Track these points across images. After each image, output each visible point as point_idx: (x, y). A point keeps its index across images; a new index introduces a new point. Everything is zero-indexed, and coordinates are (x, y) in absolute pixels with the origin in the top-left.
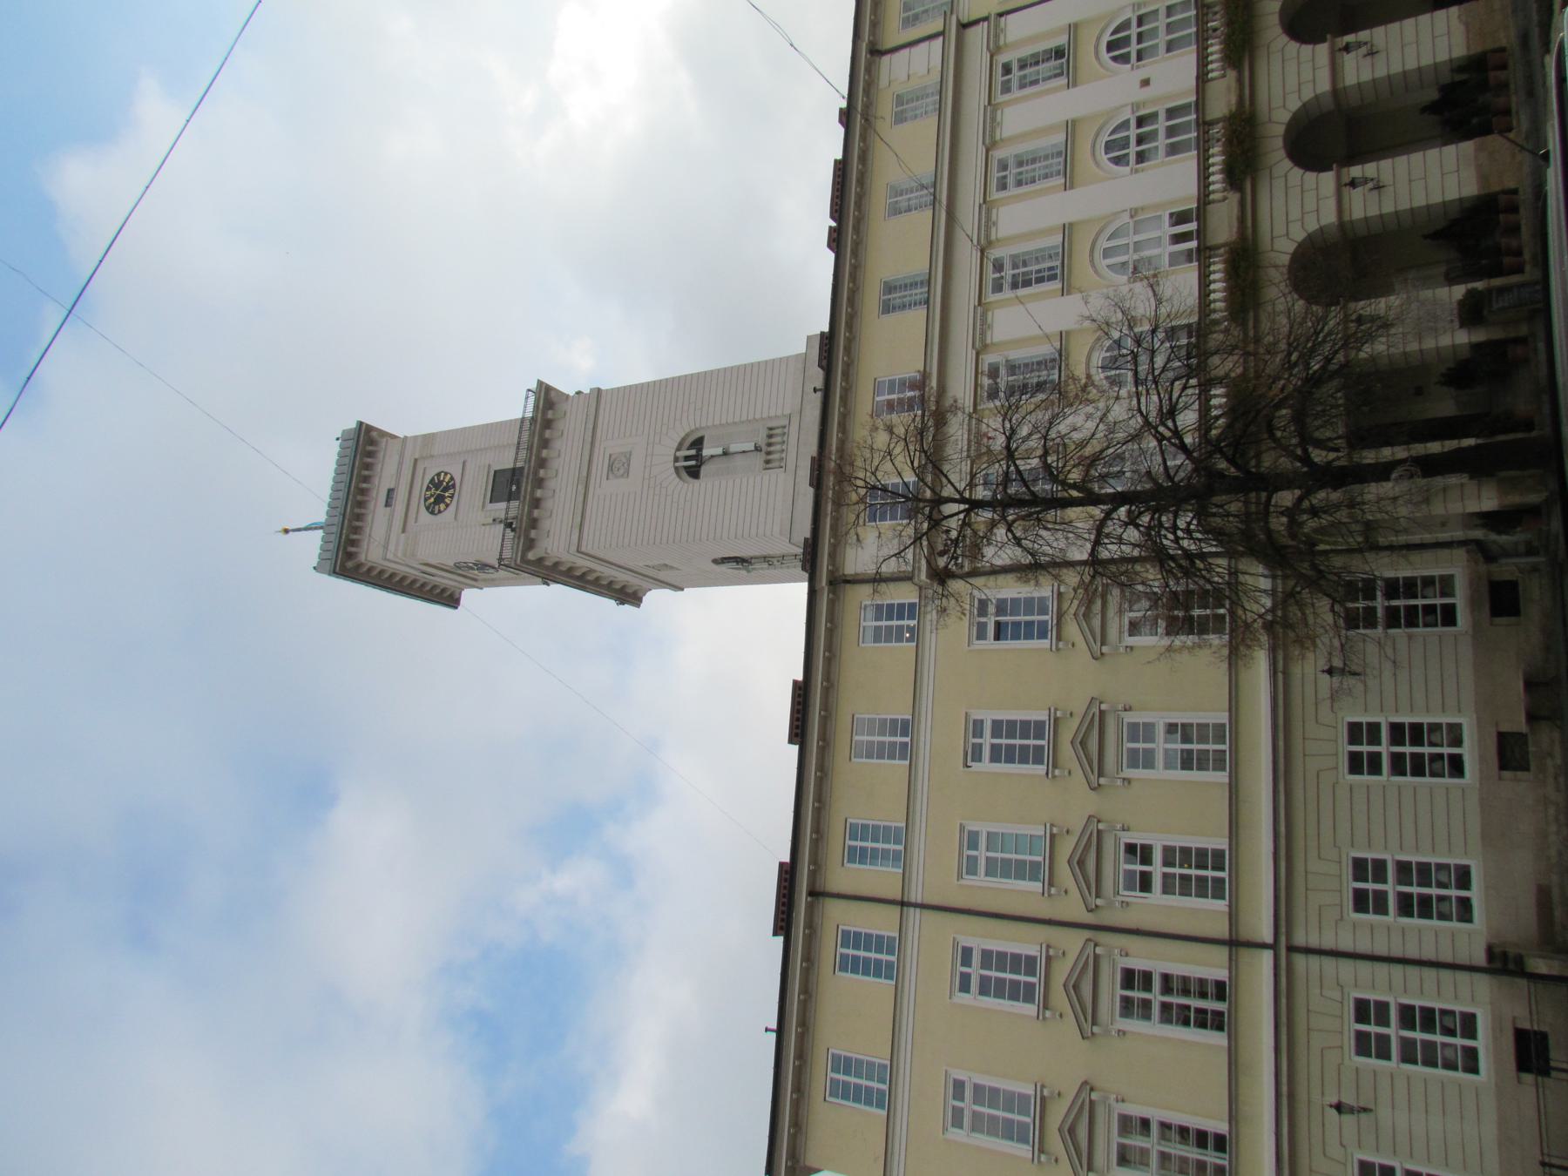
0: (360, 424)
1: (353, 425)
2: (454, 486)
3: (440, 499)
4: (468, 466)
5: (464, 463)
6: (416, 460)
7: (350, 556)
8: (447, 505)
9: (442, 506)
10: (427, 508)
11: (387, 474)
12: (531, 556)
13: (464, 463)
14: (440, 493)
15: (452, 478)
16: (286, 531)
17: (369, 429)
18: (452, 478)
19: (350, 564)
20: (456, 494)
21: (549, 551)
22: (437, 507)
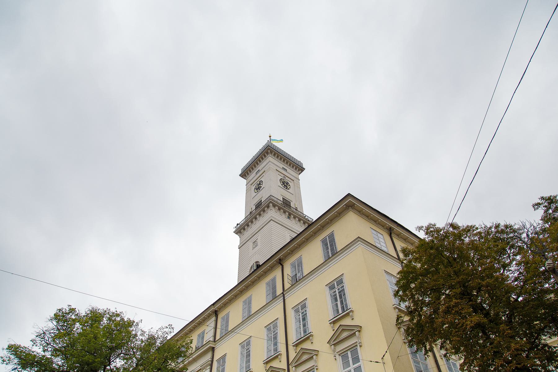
1: (304, 167)
2: (287, 189)
3: (283, 183)
5: (293, 194)
6: (293, 181)
7: (271, 153)
8: (282, 185)
10: (281, 179)
11: (291, 172)
12: (271, 205)
13: (293, 194)
14: (285, 185)
15: (289, 189)
16: (270, 137)
18: (289, 189)
19: (269, 151)
20: (284, 188)
21: (271, 210)
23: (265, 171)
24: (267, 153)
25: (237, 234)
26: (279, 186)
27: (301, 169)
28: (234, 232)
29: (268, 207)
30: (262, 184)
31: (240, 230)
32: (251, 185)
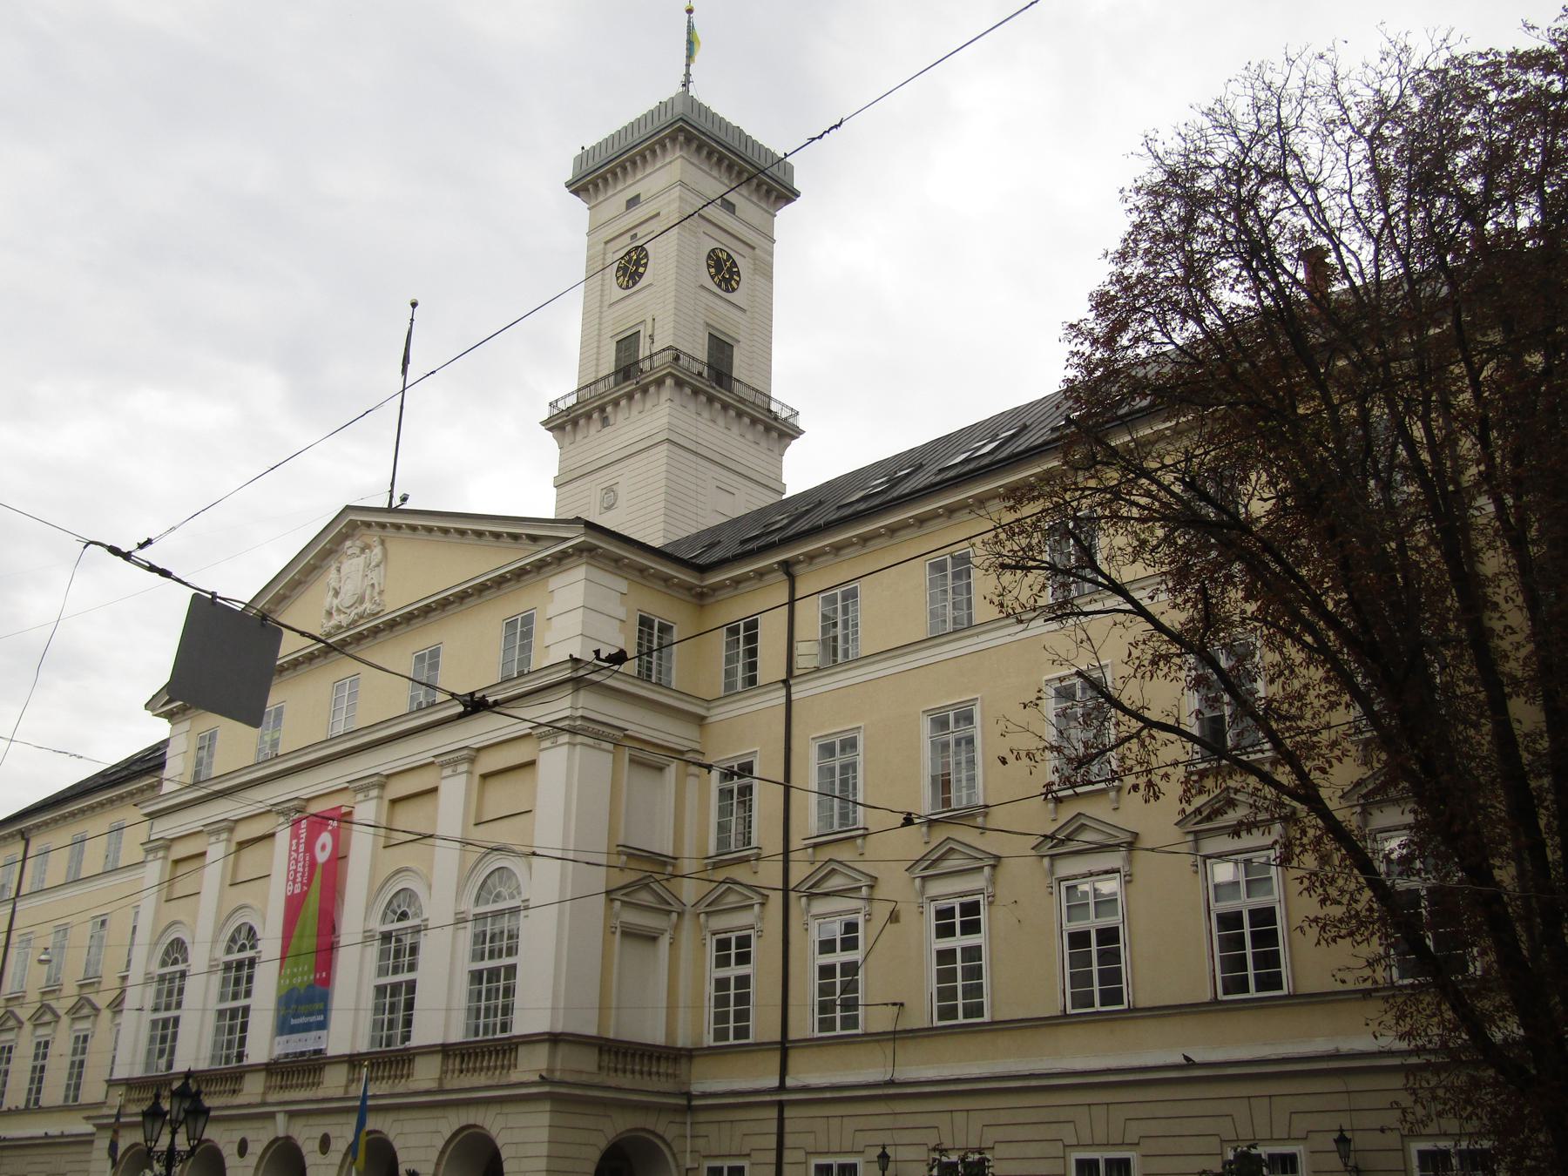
0: (797, 194)
1: (796, 186)
2: (727, 291)
4: (739, 313)
5: (743, 310)
6: (753, 248)
7: (689, 139)
8: (713, 277)
9: (712, 270)
10: (713, 251)
12: (669, 382)
13: (743, 310)
15: (734, 290)
16: (690, 11)
17: (789, 200)
19: (681, 138)
22: (712, 263)
23: (658, 214)
24: (673, 138)
25: (550, 429)
26: (702, 287)
27: (787, 195)
28: (544, 423)
29: (660, 383)
30: (646, 264)
31: (563, 423)
32: (606, 243)
